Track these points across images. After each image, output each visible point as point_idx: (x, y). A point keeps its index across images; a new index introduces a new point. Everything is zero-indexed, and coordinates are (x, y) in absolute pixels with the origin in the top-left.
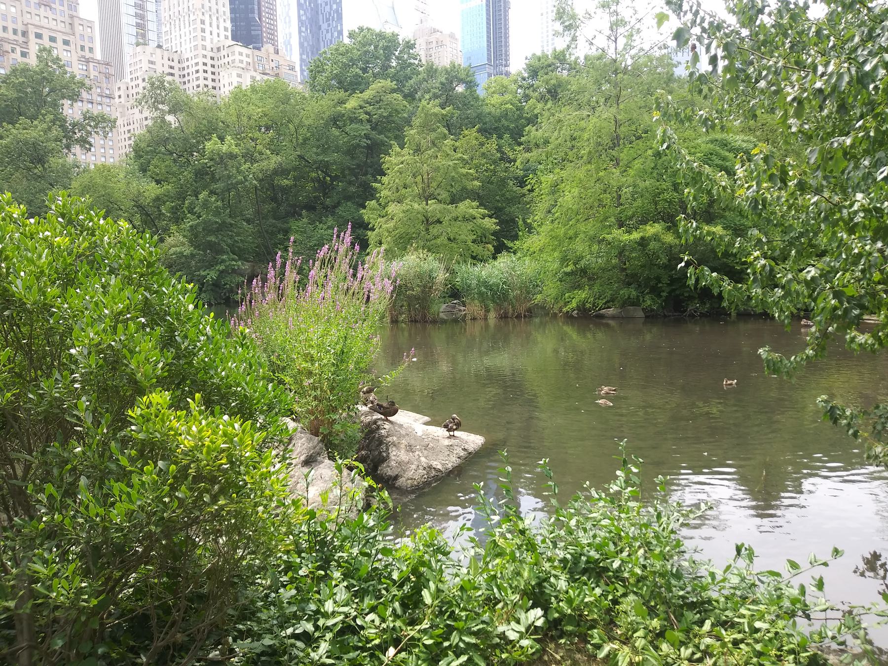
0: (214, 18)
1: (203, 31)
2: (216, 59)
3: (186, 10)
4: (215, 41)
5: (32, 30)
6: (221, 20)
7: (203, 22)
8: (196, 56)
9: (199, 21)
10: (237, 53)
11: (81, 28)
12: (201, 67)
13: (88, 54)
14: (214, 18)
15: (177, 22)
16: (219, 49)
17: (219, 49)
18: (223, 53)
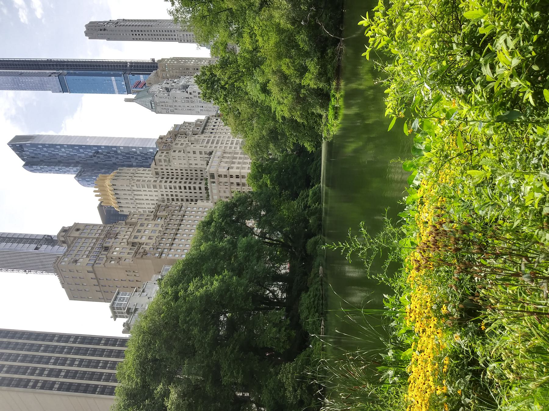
0: (137, 175)
1: (144, 181)
2: (163, 176)
3: (130, 193)
4: (152, 176)
5: (132, 240)
6: (138, 172)
7: (138, 181)
8: (160, 187)
9: (138, 183)
10: (160, 158)
11: (133, 219)
12: (168, 184)
13: (152, 217)
14: (137, 175)
15: (138, 202)
16: (157, 173)
17: (157, 173)
18: (159, 170)
